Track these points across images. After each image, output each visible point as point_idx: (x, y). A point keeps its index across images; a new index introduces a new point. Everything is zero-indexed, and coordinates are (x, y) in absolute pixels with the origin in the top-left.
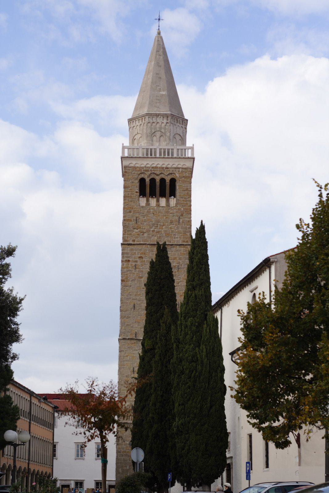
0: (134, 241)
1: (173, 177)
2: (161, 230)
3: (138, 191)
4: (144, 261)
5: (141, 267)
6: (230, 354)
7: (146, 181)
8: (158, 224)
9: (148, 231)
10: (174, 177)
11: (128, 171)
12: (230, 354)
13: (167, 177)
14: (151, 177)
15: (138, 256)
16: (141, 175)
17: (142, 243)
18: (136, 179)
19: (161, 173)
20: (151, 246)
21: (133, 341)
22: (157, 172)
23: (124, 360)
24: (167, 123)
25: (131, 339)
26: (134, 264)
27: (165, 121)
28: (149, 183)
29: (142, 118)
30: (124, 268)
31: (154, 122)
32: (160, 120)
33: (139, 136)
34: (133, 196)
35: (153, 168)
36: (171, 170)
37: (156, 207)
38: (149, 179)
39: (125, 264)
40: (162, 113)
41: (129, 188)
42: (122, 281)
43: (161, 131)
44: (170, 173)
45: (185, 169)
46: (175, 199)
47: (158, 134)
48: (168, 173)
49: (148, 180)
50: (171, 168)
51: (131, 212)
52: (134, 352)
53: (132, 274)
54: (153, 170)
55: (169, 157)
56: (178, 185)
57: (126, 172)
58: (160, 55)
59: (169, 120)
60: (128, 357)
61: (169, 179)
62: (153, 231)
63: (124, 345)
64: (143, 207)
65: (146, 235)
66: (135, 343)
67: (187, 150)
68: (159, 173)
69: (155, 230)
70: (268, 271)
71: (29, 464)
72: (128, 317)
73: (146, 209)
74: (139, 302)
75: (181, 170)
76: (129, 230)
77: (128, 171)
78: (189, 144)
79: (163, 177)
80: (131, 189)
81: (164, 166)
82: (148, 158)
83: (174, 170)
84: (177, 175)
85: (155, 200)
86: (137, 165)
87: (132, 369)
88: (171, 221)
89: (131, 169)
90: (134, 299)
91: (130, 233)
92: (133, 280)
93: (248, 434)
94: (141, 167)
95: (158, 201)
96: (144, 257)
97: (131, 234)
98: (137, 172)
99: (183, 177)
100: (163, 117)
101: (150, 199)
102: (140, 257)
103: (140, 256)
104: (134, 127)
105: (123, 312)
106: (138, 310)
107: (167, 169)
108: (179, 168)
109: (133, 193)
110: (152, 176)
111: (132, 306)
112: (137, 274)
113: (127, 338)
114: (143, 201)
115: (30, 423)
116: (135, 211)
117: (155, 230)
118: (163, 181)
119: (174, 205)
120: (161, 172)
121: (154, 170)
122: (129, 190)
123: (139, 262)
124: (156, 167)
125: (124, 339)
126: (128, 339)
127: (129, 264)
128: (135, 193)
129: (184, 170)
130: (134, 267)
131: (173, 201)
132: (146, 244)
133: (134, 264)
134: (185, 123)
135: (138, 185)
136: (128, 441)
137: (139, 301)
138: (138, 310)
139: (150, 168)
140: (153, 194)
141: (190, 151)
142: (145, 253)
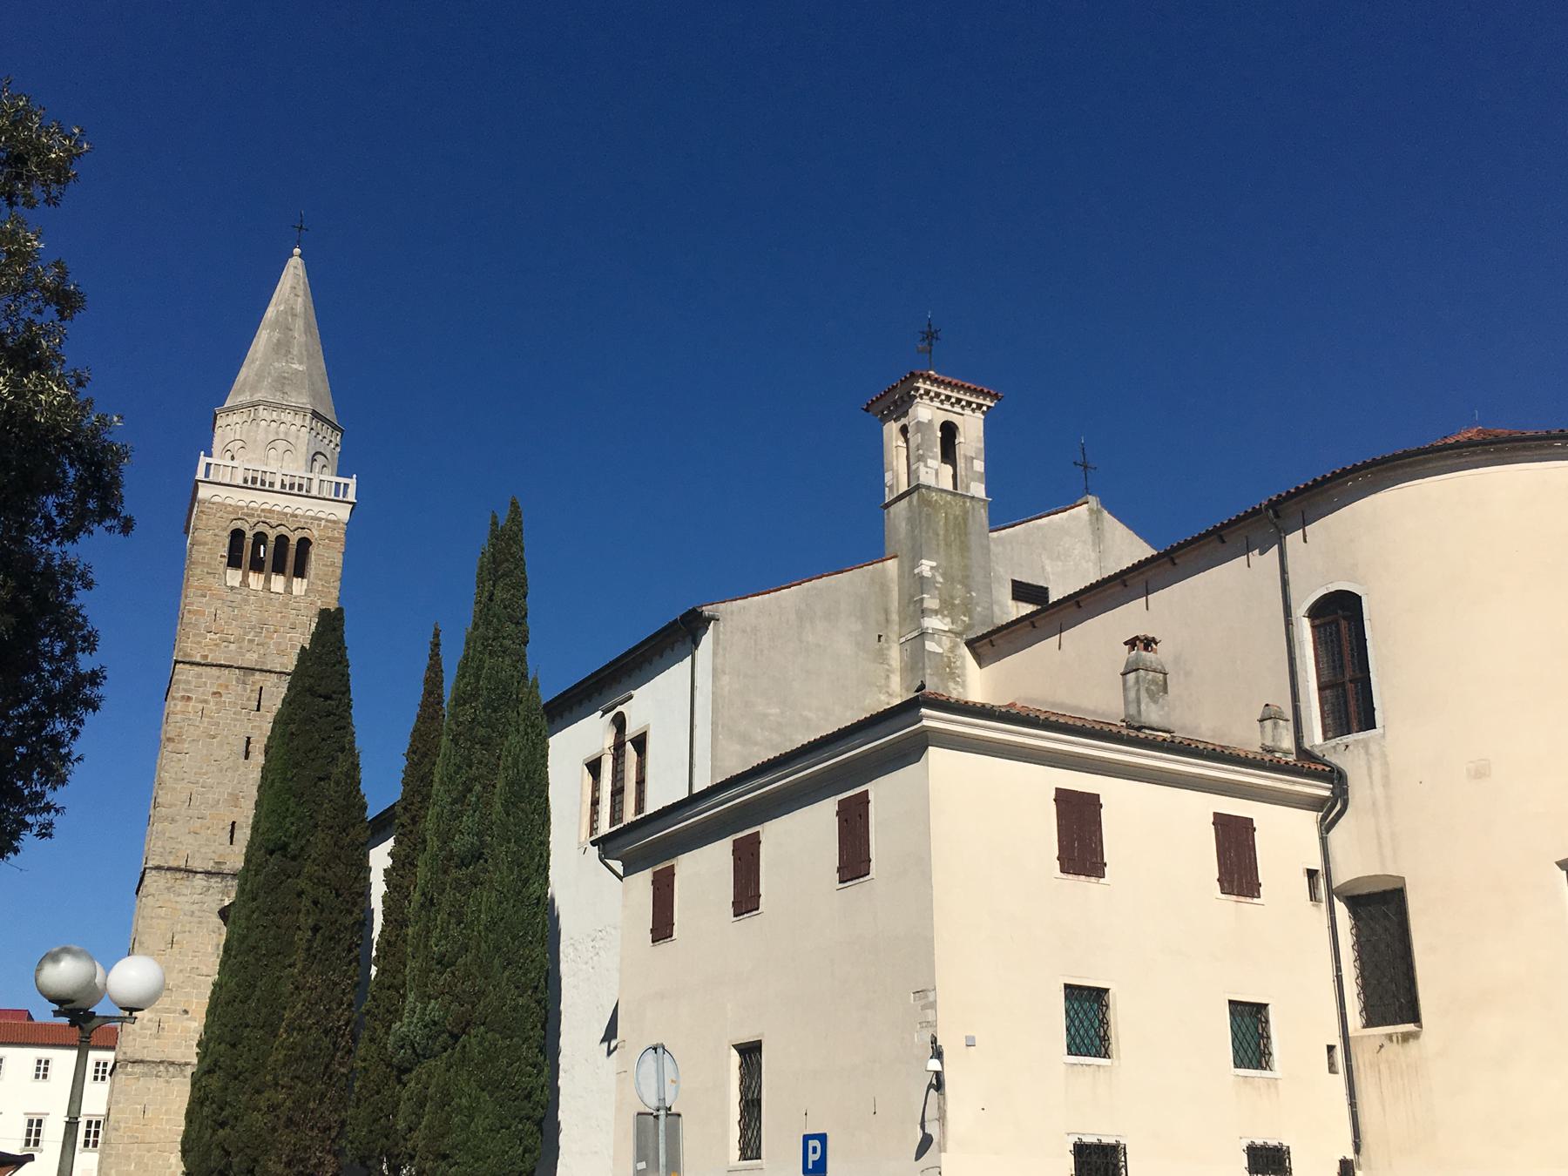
0: (206, 657)
1: (305, 535)
2: (268, 640)
4: (225, 702)
9: (240, 640)
14: (258, 529)
16: (234, 521)
17: (222, 662)
18: (225, 529)
20: (242, 673)
21: (178, 875)
25: (178, 869)
26: (200, 706)
27: (299, 422)
28: (252, 541)
32: (287, 417)
34: (213, 563)
35: (263, 510)
36: (302, 520)
40: (293, 404)
41: (207, 547)
45: (334, 522)
46: (305, 581)
47: (281, 445)
48: (295, 526)
49: (249, 535)
50: (302, 516)
51: (205, 597)
52: (178, 899)
56: (314, 552)
58: (297, 295)
62: (251, 641)
64: (232, 588)
65: (232, 647)
68: (276, 524)
75: (323, 523)
77: (209, 510)
80: (211, 549)
81: (287, 510)
83: (310, 521)
84: (316, 533)
85: (262, 577)
86: (228, 501)
88: (292, 624)
92: (193, 740)
94: (238, 506)
95: (268, 580)
97: (200, 642)
99: (328, 538)
101: (251, 574)
102: (214, 693)
103: (215, 690)
108: (320, 519)
109: (215, 556)
110: (261, 528)
111: (185, 796)
114: (234, 577)
116: (214, 595)
118: (282, 540)
119: (303, 594)
120: (280, 522)
121: (265, 517)
124: (270, 511)
126: (169, 869)
127: (188, 706)
128: (219, 558)
130: (200, 713)
131: (299, 586)
132: (231, 666)
133: (200, 706)
135: (227, 541)
136: (139, 1104)
137: (202, 787)
139: (257, 510)
140: (257, 566)
142: (227, 687)
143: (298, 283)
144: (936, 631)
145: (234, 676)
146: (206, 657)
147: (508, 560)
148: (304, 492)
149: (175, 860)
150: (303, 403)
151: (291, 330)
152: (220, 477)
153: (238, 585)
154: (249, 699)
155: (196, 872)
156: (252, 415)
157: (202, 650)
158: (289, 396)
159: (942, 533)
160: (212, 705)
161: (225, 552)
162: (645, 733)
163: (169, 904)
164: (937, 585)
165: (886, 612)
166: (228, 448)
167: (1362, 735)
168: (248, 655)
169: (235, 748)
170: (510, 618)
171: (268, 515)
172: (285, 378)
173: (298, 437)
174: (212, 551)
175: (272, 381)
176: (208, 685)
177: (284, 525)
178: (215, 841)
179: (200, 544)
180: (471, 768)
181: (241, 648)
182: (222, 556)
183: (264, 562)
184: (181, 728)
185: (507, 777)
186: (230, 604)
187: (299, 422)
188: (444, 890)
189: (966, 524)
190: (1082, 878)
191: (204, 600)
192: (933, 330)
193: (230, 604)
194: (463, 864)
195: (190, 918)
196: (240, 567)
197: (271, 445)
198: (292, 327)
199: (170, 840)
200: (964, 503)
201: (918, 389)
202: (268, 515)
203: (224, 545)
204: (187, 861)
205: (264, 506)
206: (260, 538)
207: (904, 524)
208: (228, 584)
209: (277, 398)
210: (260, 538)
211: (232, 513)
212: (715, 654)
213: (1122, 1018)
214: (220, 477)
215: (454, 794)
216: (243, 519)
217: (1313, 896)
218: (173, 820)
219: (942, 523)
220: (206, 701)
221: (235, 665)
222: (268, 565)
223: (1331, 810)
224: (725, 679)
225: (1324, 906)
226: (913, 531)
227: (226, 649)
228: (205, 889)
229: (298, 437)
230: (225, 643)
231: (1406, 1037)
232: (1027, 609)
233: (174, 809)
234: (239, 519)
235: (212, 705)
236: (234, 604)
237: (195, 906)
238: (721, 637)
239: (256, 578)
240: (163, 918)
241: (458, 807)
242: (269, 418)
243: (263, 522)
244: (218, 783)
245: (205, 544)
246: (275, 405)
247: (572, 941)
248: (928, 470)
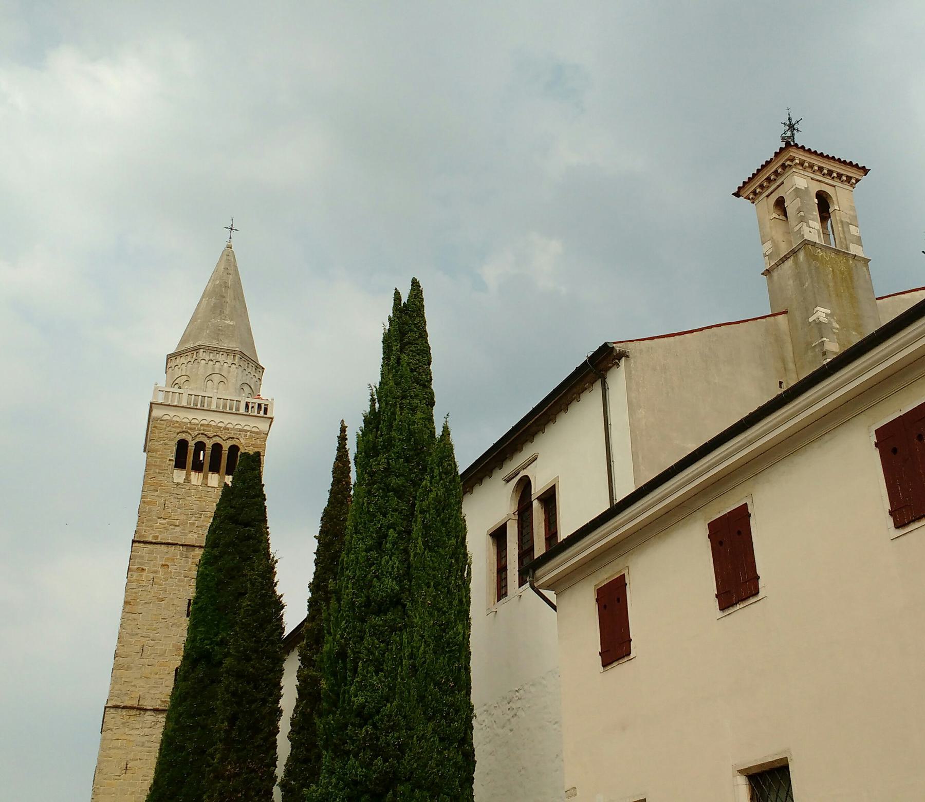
0: (157, 537)
1: (235, 443)
3: (173, 458)
4: (171, 572)
5: (164, 582)
7: (188, 444)
8: (201, 514)
9: (183, 524)
10: (236, 444)
11: (160, 426)
13: (225, 442)
14: (198, 440)
15: (161, 563)
17: (170, 541)
19: (216, 436)
22: (208, 433)
23: (111, 746)
24: (232, 364)
26: (152, 575)
27: (230, 361)
28: (194, 448)
29: (192, 352)
30: (133, 582)
31: (211, 360)
33: (185, 378)
35: (202, 425)
36: (233, 432)
37: (201, 487)
38: (194, 442)
39: (135, 576)
41: (158, 453)
42: (126, 603)
43: (221, 375)
44: (231, 436)
45: (257, 433)
47: (217, 378)
49: (192, 444)
50: (233, 429)
52: (131, 732)
53: (146, 593)
54: (202, 428)
55: (231, 411)
59: (237, 360)
60: (120, 741)
61: (229, 446)
63: (114, 718)
64: (178, 484)
65: (178, 529)
66: (135, 715)
68: (212, 435)
69: (195, 523)
70: (598, 387)
72: (128, 668)
73: (183, 488)
74: (153, 642)
75: (248, 434)
76: (150, 520)
77: (160, 426)
79: (218, 442)
81: (220, 425)
82: (196, 409)
84: (242, 441)
85: (201, 475)
86: (176, 419)
87: (123, 764)
89: (165, 423)
90: (144, 637)
91: (151, 523)
92: (146, 603)
93: (741, 772)
94: (183, 422)
95: (205, 477)
96: (172, 565)
98: (175, 429)
100: (228, 355)
101: (193, 473)
102: (163, 565)
103: (163, 563)
104: (177, 367)
105: (121, 659)
106: (149, 656)
107: (226, 431)
111: (138, 648)
112: (155, 593)
113: (122, 705)
114: (179, 476)
117: (195, 523)
118: (217, 448)
120: (215, 434)
122: (157, 456)
123: (161, 573)
125: (116, 707)
126: (124, 707)
127: (142, 576)
129: (254, 435)
130: (152, 581)
132: (176, 544)
133: (152, 575)
134: (259, 372)
135: (175, 448)
137: (152, 640)
138: (149, 656)
140: (198, 467)
143: (230, 265)
145: (179, 551)
146: (157, 537)
147: (411, 330)
148: (234, 411)
149: (130, 699)
150: (232, 348)
151: (224, 297)
152: (170, 400)
153: (182, 482)
154: (190, 570)
155: (146, 710)
156: (195, 356)
157: (153, 532)
158: (223, 342)
159: (831, 284)
160: (161, 575)
161: (172, 456)
162: (554, 486)
163: (124, 737)
164: (834, 330)
165: (784, 361)
166: (176, 382)
168: (190, 535)
169: (179, 608)
170: (417, 381)
171: (207, 428)
172: (219, 330)
173: (229, 372)
174: (163, 456)
175: (210, 332)
176: (158, 559)
177: (218, 436)
178: (162, 684)
179: (154, 451)
180: (385, 515)
181: (184, 529)
182: (170, 460)
183: (203, 464)
184: (136, 593)
185: (423, 521)
186: (176, 496)
187: (230, 361)
188: (362, 639)
189: (851, 278)
191: (156, 493)
192: (793, 122)
193: (176, 496)
194: (380, 610)
195: (140, 748)
196: (185, 469)
197: (209, 379)
198: (225, 295)
199: (126, 684)
200: (848, 260)
201: (792, 159)
202: (207, 428)
203: (172, 452)
204: (139, 700)
205: (202, 422)
206: (200, 446)
207: (791, 282)
208: (175, 482)
209: (214, 344)
210: (200, 446)
211: (179, 428)
212: (629, 388)
214: (170, 400)
215: (370, 542)
216: (187, 432)
218: (128, 667)
219: (830, 276)
220: (156, 572)
221: (180, 543)
222: (206, 466)
224: (641, 413)
226: (802, 285)
227: (172, 531)
228: (153, 723)
229: (229, 372)
230: (172, 527)
233: (128, 659)
234: (183, 432)
235: (161, 575)
236: (179, 496)
237: (146, 738)
238: (633, 372)
239: (197, 476)
240: (119, 748)
241: (374, 554)
242: (207, 358)
243: (202, 434)
244: (165, 637)
245: (156, 451)
246: (212, 349)
247: (485, 708)
248: (811, 229)
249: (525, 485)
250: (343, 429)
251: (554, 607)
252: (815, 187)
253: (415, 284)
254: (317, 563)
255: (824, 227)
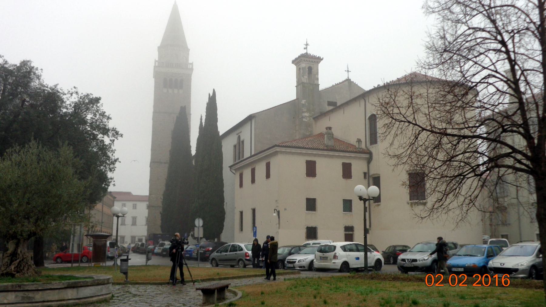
6: (229, 167)
12: (229, 167)
57: (157, 75)
67: (189, 65)
71: (101, 228)
78: (190, 62)
114: (165, 91)
115: (103, 205)
141: (191, 65)
144: (306, 116)
167: (375, 145)
190: (311, 177)
213: (319, 205)
217: (365, 177)
223: (369, 161)
225: (367, 180)
231: (378, 205)
232: (331, 108)
249: (239, 137)
250: (201, 117)
251: (235, 174)
252: (308, 65)
253: (214, 90)
254: (196, 150)
255: (309, 77)
